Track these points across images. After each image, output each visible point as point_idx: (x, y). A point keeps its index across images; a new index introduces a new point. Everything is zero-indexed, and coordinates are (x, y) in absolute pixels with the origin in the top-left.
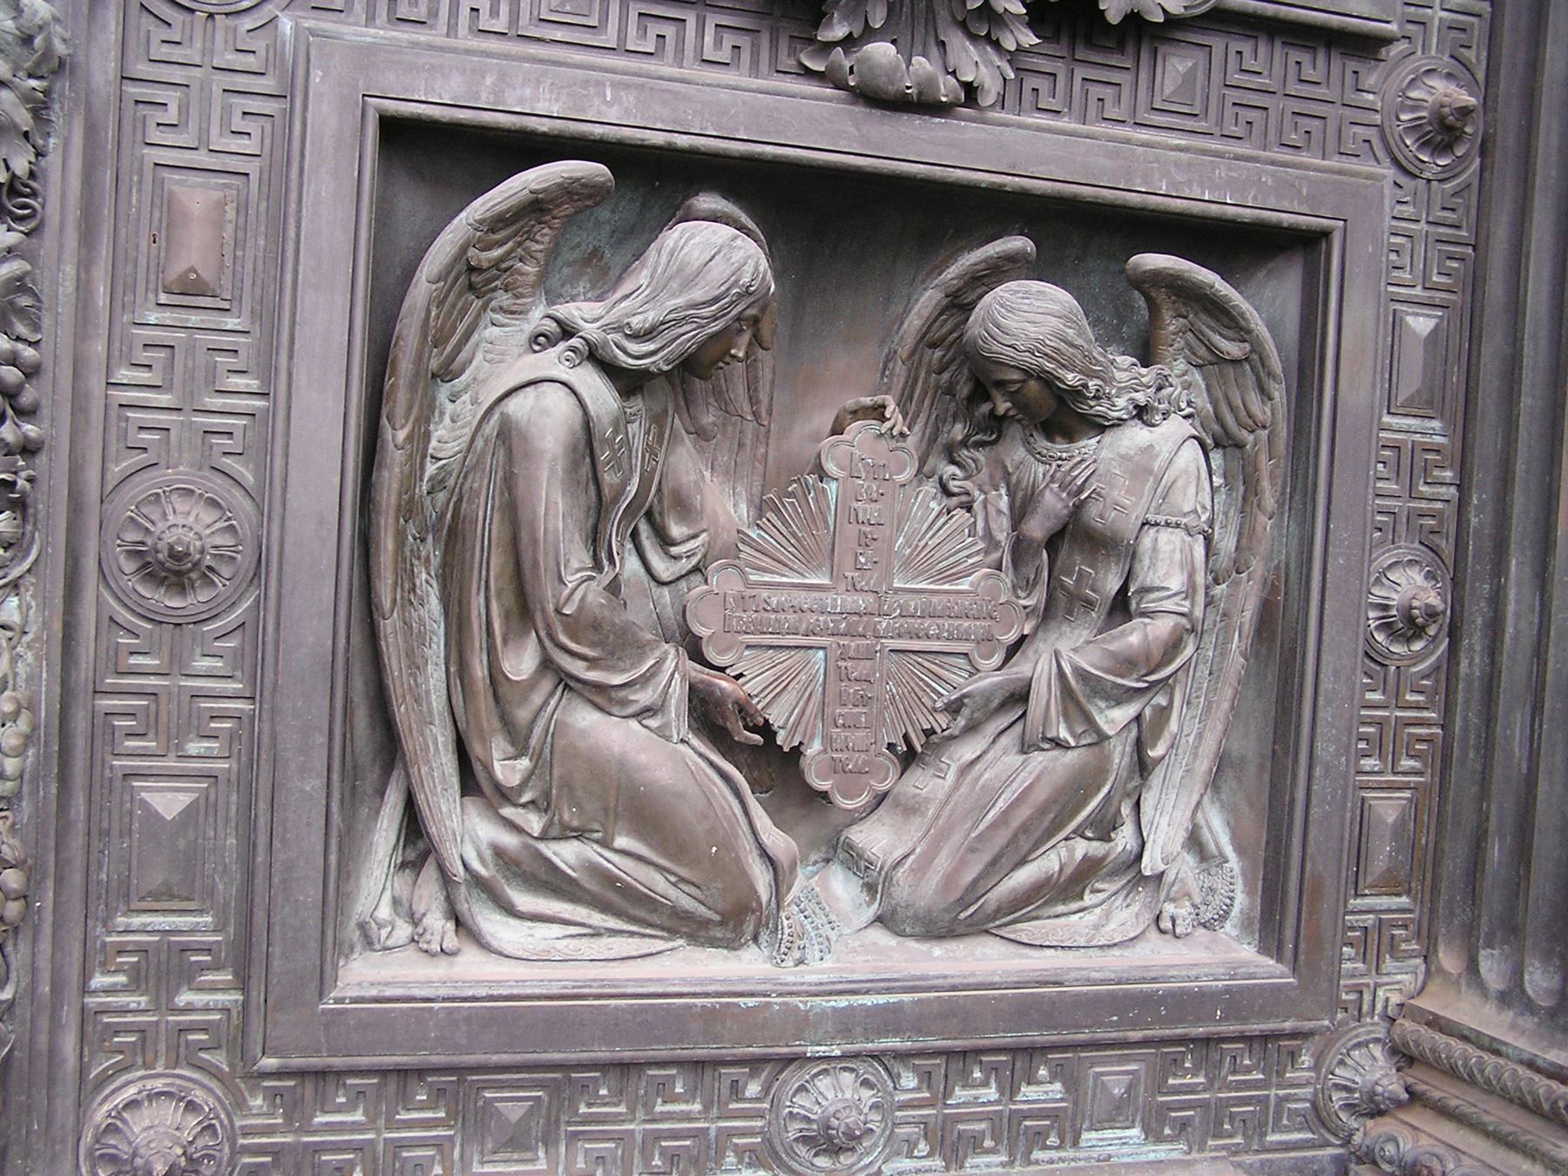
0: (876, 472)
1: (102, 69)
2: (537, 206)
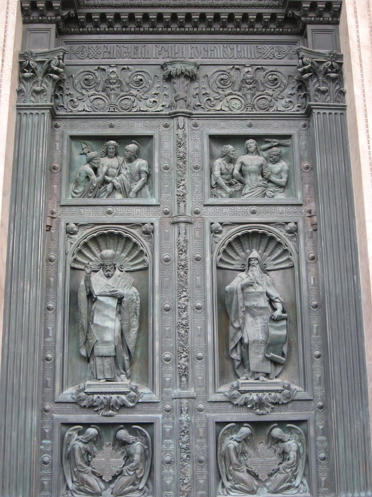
0: (263, 448)
1: (193, 421)
2: (229, 428)
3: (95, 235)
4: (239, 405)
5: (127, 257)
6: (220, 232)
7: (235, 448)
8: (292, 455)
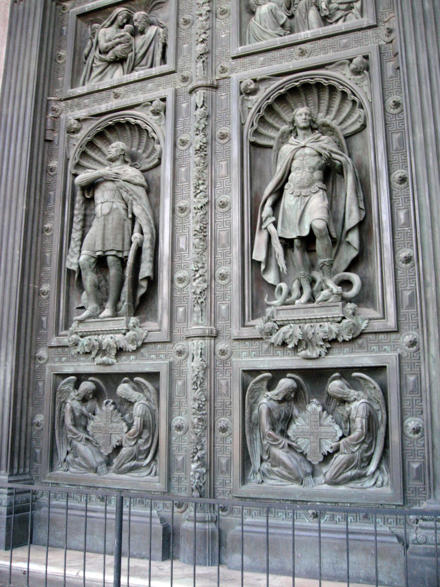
2: (262, 379)
3: (99, 129)
4: (276, 345)
5: (144, 152)
6: (254, 92)
7: (270, 411)
8: (359, 424)
